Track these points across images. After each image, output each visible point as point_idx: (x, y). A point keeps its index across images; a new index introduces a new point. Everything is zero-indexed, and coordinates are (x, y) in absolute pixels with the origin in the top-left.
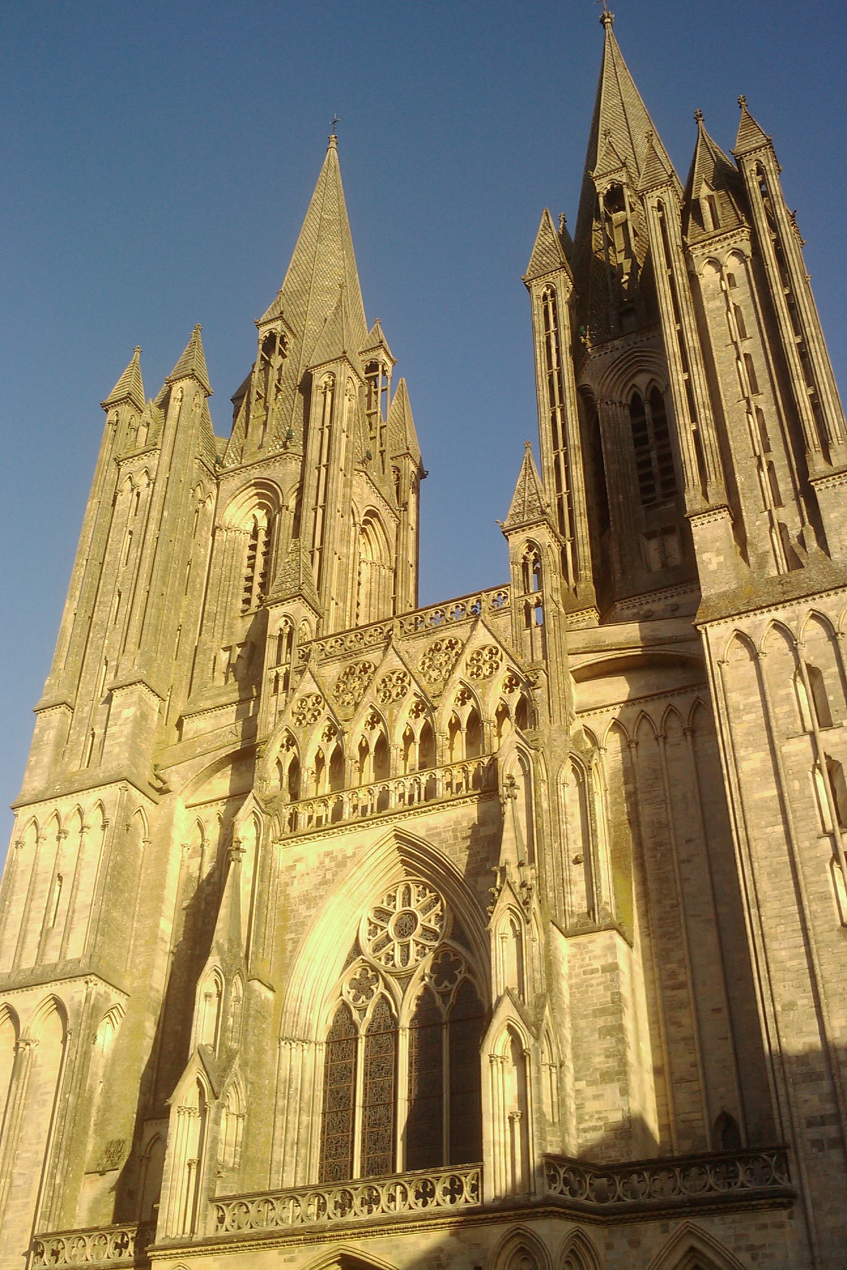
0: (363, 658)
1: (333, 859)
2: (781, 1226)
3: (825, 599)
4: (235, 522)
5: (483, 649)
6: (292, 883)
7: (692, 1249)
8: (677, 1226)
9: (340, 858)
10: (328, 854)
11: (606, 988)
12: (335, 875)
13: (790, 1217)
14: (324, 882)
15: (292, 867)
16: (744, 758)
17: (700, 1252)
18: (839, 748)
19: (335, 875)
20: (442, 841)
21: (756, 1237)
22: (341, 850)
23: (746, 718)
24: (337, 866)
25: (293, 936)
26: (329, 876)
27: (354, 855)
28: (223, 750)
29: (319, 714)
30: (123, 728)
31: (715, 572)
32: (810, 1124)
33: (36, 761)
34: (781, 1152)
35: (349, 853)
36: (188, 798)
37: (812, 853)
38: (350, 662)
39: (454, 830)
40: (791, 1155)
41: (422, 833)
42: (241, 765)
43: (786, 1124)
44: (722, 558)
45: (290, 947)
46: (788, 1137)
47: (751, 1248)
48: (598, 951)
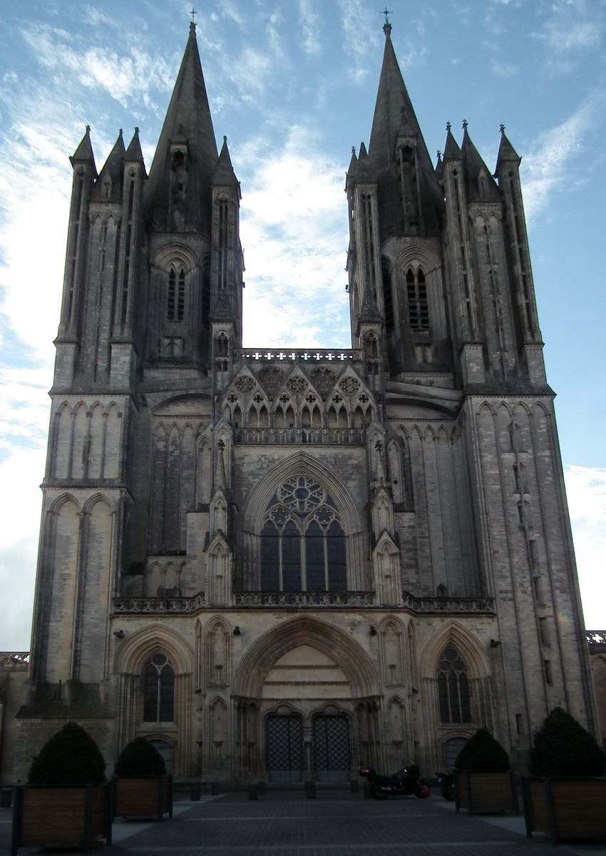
1: (266, 459)
2: (489, 624)
3: (527, 398)
5: (350, 378)
6: (243, 465)
7: (452, 628)
8: (447, 620)
9: (270, 459)
10: (263, 456)
11: (410, 534)
12: (268, 466)
13: (493, 621)
14: (262, 468)
15: (243, 458)
16: (483, 456)
17: (456, 630)
18: (527, 461)
19: (268, 466)
20: (328, 462)
21: (479, 627)
22: (271, 456)
23: (485, 440)
24: (270, 462)
25: (245, 489)
26: (265, 466)
27: (278, 459)
29: (252, 387)
31: (475, 373)
32: (501, 592)
34: (491, 600)
35: (276, 457)
37: (510, 499)
39: (335, 458)
40: (494, 601)
41: (317, 456)
43: (493, 591)
44: (479, 368)
45: (244, 493)
46: (494, 596)
47: (477, 630)
48: (407, 520)
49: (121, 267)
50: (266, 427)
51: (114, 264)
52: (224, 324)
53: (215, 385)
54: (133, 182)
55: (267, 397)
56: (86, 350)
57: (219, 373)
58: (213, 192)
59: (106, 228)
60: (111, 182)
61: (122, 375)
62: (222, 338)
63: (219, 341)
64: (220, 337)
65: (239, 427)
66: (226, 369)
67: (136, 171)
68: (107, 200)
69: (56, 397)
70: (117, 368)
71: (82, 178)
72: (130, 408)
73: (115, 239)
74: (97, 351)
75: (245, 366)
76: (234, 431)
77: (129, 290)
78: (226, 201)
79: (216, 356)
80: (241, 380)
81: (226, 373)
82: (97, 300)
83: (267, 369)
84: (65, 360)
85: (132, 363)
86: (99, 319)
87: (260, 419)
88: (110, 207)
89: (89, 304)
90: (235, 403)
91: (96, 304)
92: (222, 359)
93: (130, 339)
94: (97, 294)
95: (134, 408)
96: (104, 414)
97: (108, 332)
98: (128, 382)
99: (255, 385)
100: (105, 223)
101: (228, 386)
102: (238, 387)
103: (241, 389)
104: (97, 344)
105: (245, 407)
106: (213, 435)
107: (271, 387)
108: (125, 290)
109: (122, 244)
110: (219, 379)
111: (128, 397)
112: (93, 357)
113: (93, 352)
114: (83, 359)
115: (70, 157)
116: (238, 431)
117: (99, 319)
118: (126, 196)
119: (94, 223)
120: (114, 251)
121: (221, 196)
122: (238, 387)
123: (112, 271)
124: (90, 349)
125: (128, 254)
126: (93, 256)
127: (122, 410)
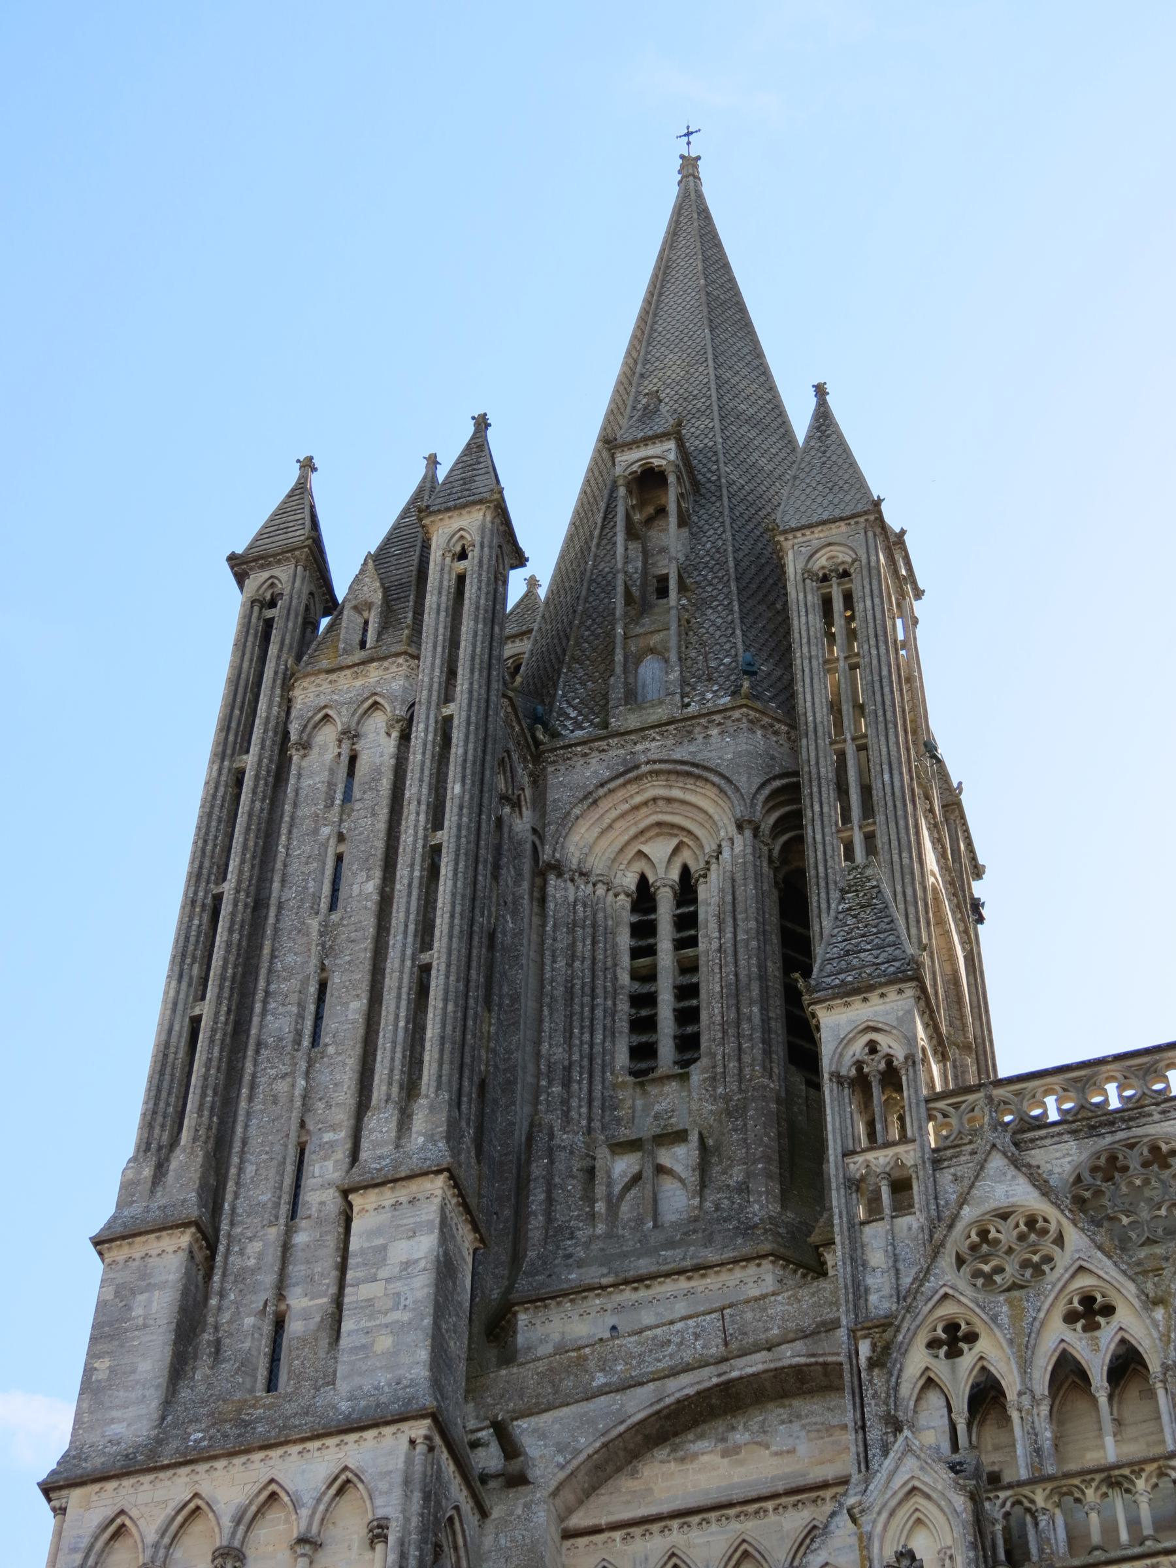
0: (1151, 1130)
4: (597, 864)
28: (685, 1379)
29: (1048, 1259)
30: (398, 1286)
33: (112, 1370)
36: (570, 1511)
38: (1109, 1139)
42: (733, 1428)
49: (408, 872)
50: (1157, 1451)
51: (378, 873)
52: (874, 997)
53: (859, 1291)
54: (461, 579)
55: (1130, 1288)
56: (242, 1253)
57: (868, 1230)
58: (790, 558)
59: (353, 759)
60: (377, 597)
61: (396, 1329)
62: (877, 1065)
63: (860, 1083)
64: (859, 1065)
65: (1007, 1478)
66: (902, 1206)
67: (473, 536)
68: (359, 655)
69: (75, 1496)
70: (370, 1302)
71: (269, 613)
72: (432, 1494)
73: (386, 784)
74: (286, 1247)
75: (997, 1162)
76: (975, 1498)
77: (437, 956)
78: (846, 574)
79: (847, 1154)
80: (983, 1234)
81: (912, 1223)
82: (299, 1034)
83: (1113, 1159)
84: (138, 1312)
85: (445, 1269)
86: (306, 1108)
87: (1118, 1422)
88: (374, 673)
89: (265, 1053)
90: (968, 1360)
91: (297, 1042)
92: (880, 1159)
93: (440, 1152)
94: (301, 1006)
95: (458, 1493)
96: (302, 1540)
97: (341, 1154)
98: (423, 1355)
99: (1060, 1241)
100: (351, 735)
101: (922, 1279)
102: (977, 1274)
103: (989, 1278)
104: (293, 1214)
105: (1025, 1366)
106: (864, 1541)
107: (1150, 1242)
108: (424, 958)
109: (416, 790)
110: (877, 1257)
111: (420, 1429)
112: (268, 1279)
113: (273, 1256)
114: (222, 1295)
115: (233, 559)
116: (995, 1509)
117: (306, 1108)
118: (433, 622)
119: (306, 746)
120: (382, 826)
121: (822, 561)
122: (977, 1274)
123: (372, 905)
124: (254, 1247)
125: (437, 823)
126: (295, 866)
127: (390, 1505)
